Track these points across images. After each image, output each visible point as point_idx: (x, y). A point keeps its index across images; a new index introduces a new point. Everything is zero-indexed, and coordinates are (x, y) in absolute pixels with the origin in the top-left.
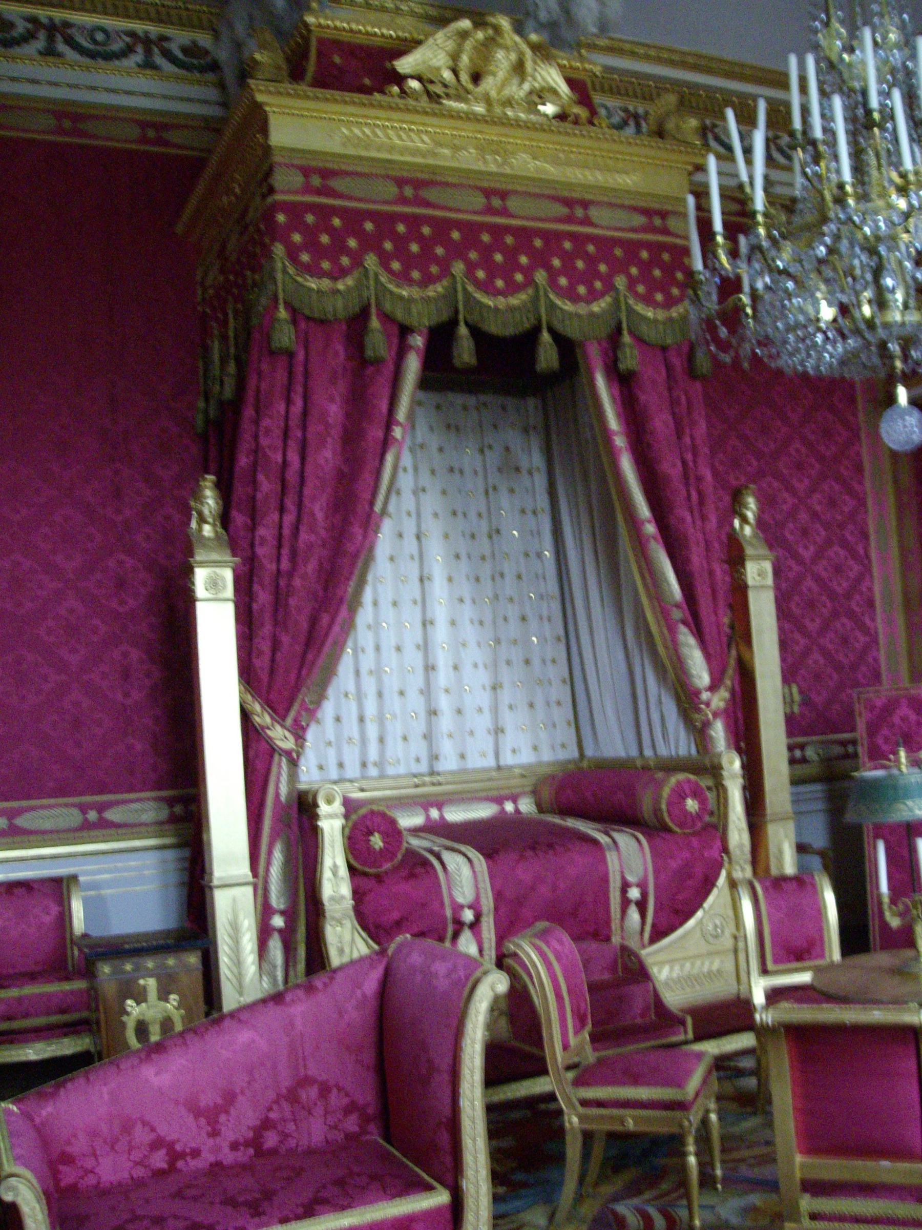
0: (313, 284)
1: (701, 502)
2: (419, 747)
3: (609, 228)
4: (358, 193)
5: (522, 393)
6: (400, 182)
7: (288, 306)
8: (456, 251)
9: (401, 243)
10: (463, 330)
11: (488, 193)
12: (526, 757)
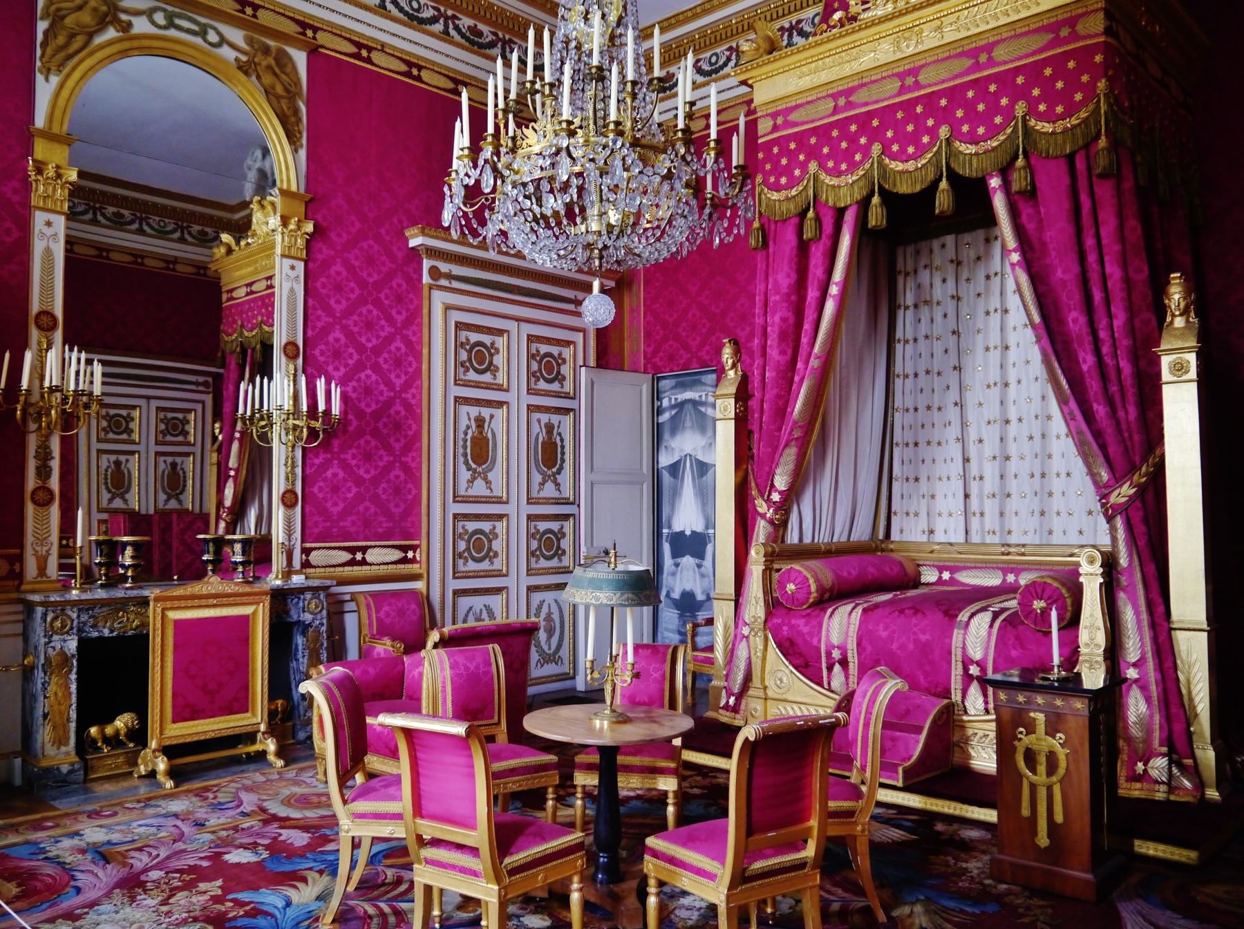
1: (1107, 302)
3: (1012, 61)
4: (804, 119)
6: (835, 96)
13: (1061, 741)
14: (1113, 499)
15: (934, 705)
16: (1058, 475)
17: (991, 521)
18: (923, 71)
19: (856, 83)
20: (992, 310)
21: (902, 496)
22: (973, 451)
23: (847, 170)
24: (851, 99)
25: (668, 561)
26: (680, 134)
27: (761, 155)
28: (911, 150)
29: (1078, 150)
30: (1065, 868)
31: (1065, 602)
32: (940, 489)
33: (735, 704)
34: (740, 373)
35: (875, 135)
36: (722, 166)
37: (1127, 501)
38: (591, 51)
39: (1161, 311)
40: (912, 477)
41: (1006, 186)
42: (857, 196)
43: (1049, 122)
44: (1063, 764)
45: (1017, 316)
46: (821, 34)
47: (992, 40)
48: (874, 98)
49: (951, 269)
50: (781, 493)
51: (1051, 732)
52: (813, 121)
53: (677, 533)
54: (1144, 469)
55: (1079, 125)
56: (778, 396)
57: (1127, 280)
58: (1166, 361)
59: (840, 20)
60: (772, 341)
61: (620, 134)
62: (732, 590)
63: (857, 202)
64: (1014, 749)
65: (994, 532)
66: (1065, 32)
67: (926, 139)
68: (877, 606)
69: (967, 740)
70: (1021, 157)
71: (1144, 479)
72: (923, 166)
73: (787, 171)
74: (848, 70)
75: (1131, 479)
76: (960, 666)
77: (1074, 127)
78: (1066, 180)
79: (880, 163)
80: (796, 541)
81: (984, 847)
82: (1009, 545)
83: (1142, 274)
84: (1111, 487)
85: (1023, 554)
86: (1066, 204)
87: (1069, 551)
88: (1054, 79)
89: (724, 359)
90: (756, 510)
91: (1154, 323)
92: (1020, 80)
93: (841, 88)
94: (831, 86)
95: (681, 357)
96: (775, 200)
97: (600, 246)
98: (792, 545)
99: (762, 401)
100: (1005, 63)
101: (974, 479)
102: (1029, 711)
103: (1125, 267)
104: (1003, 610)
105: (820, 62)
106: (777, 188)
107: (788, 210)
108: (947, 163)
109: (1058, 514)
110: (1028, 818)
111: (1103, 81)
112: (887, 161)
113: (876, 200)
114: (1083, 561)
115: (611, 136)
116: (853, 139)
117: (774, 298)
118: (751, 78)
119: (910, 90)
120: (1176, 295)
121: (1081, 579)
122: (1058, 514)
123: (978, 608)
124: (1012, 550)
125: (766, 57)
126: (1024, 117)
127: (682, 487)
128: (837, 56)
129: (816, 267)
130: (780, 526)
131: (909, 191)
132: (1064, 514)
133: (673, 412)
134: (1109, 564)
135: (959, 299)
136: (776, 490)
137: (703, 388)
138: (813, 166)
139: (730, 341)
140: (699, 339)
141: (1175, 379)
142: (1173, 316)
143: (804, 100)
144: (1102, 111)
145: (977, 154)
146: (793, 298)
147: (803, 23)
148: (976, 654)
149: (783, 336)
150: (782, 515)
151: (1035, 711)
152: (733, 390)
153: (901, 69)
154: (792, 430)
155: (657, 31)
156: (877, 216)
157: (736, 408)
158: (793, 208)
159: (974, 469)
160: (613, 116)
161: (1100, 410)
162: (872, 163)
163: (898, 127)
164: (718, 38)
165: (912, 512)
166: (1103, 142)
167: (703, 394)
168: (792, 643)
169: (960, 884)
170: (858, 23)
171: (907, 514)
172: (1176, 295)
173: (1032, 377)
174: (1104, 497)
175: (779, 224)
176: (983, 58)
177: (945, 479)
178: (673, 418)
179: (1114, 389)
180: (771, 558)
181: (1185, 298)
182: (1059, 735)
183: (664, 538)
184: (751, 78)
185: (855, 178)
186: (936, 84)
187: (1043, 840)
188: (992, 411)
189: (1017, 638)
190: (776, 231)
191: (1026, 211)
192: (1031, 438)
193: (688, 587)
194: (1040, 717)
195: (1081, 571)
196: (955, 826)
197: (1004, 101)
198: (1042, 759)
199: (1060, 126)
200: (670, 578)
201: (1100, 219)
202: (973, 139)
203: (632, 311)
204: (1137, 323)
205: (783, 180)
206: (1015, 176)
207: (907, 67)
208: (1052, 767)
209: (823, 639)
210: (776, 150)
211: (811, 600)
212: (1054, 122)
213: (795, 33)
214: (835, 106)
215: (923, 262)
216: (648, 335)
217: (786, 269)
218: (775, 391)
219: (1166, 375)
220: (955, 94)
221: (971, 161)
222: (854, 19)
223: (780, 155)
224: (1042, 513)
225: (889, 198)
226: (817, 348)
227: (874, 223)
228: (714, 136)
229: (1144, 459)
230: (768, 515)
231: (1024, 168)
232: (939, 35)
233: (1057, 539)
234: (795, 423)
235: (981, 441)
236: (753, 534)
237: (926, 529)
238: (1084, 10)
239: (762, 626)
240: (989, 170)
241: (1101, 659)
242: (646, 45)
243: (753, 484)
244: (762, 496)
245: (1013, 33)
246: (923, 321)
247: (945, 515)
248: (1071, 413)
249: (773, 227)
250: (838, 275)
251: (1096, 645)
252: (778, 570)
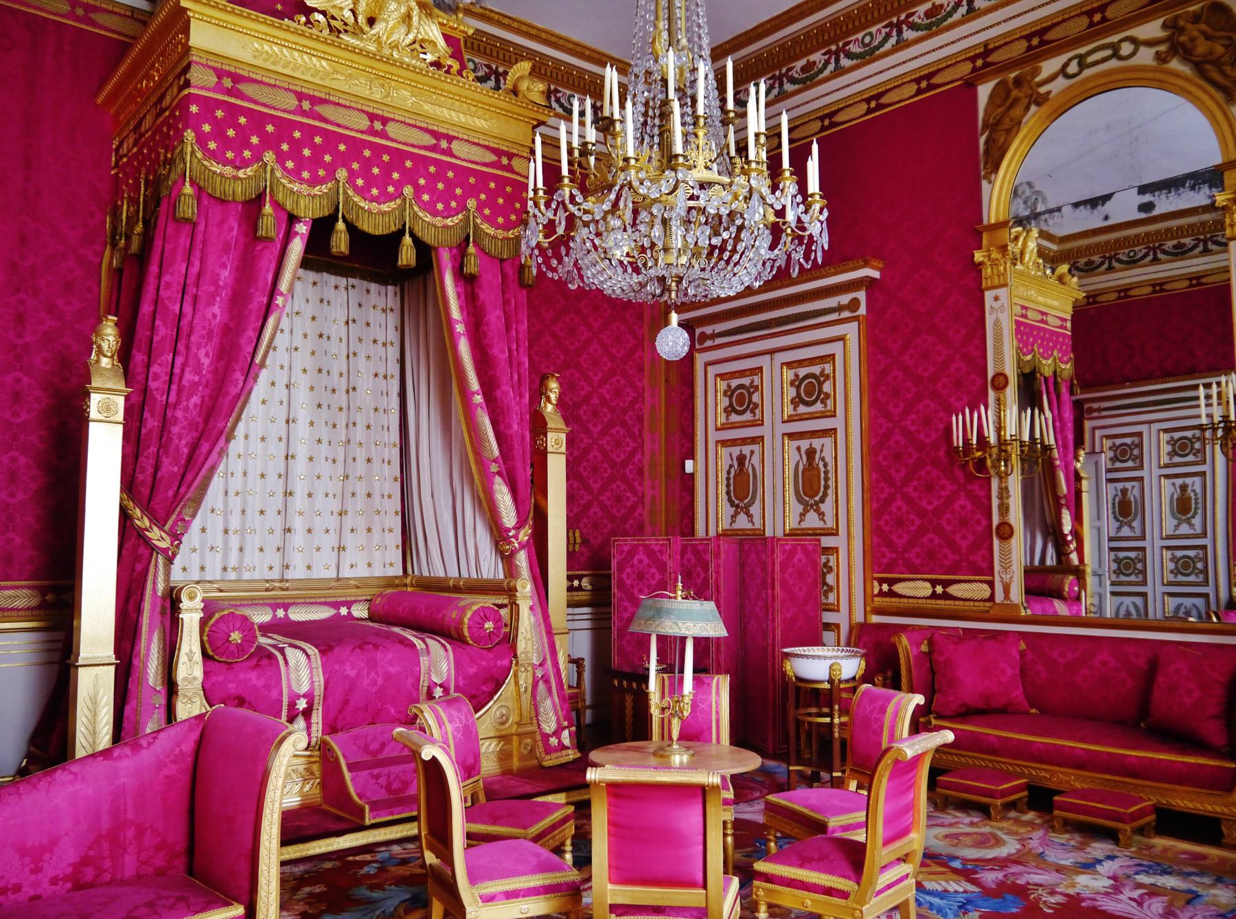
0: (217, 168)
2: (275, 559)
5: (383, 280)
6: (300, 96)
7: (192, 183)
8: (342, 160)
9: (296, 146)
10: (341, 225)
11: (372, 117)
12: (362, 572)
28: (375, 192)
85: (287, 589)
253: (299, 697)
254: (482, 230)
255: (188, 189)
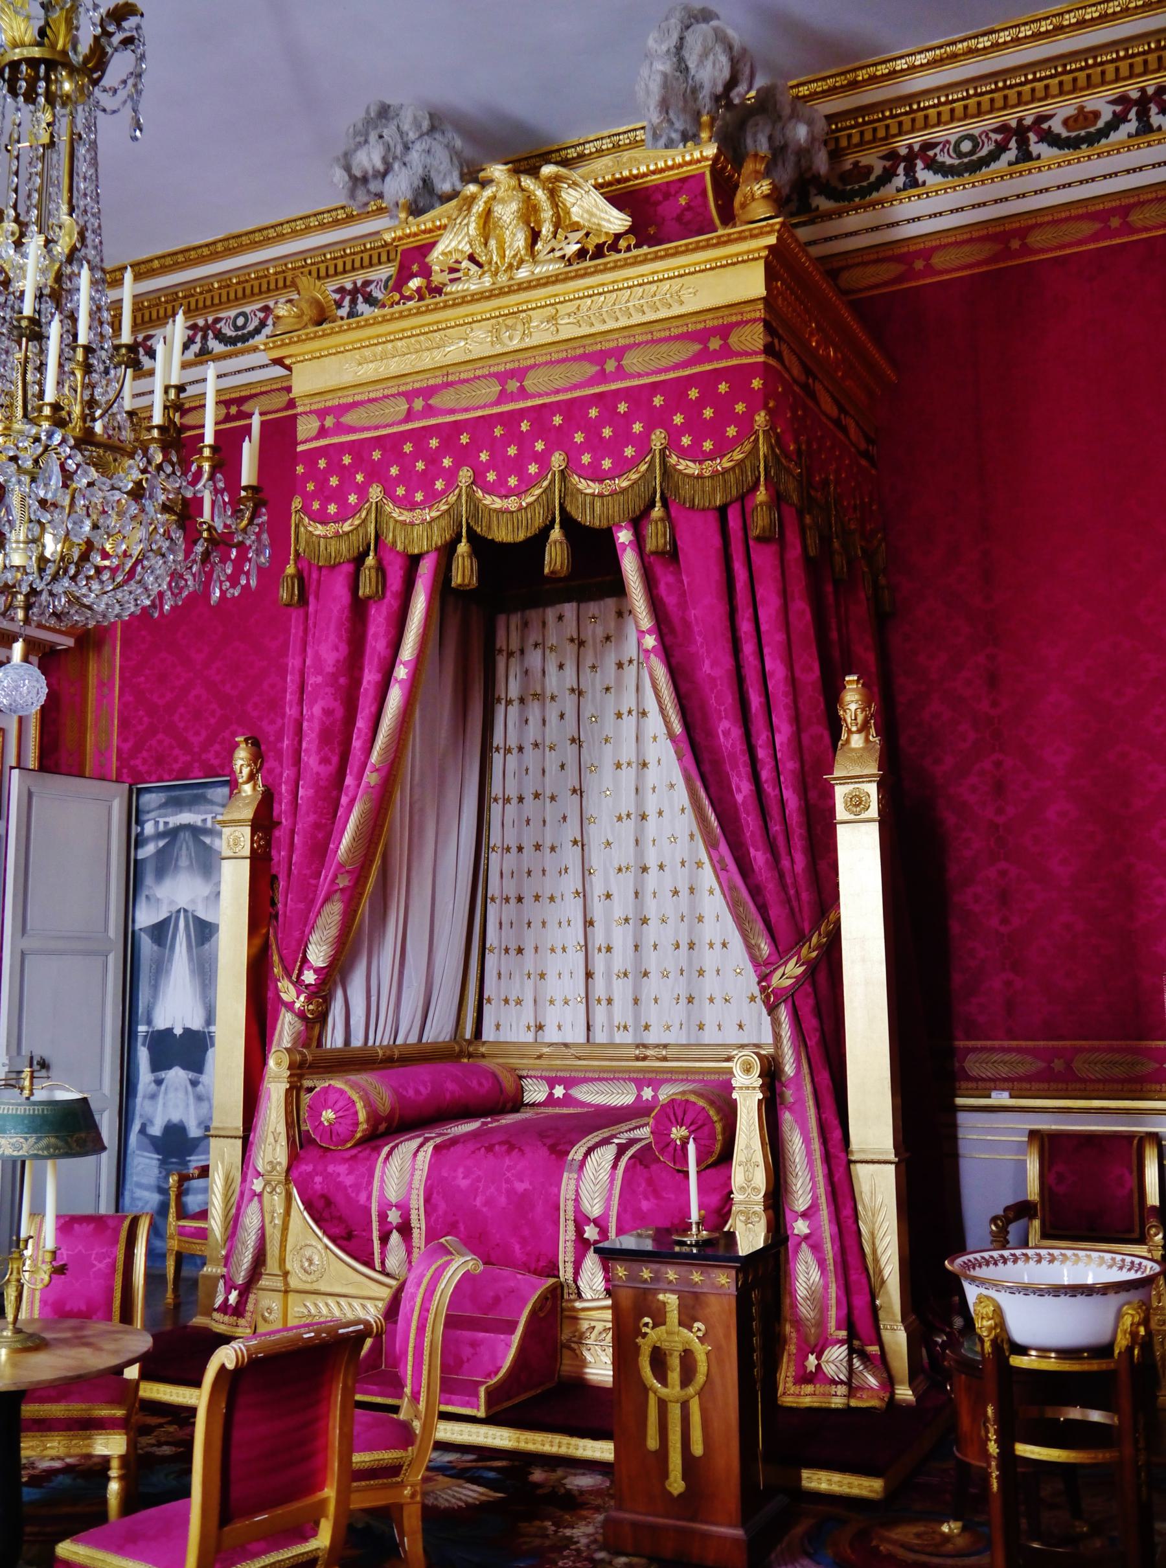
3: (648, 374)
6: (409, 396)
13: (700, 1334)
14: (777, 981)
15: (535, 1289)
16: (711, 945)
17: (622, 1011)
18: (531, 374)
19: (439, 381)
20: (625, 711)
21: (499, 975)
22: (598, 910)
23: (422, 502)
24: (431, 402)
25: (145, 1076)
26: (155, 433)
27: (300, 469)
28: (513, 481)
29: (731, 503)
30: (707, 1522)
31: (713, 1128)
32: (553, 964)
33: (238, 1303)
34: (260, 789)
35: (464, 456)
36: (221, 485)
37: (793, 984)
38: (22, 293)
39: (835, 725)
40: (513, 947)
41: (639, 542)
42: (438, 540)
43: (694, 462)
44: (702, 1368)
45: (654, 724)
46: (392, 306)
47: (622, 342)
48: (464, 404)
49: (571, 649)
50: (317, 971)
51: (686, 1321)
52: (377, 428)
53: (160, 1032)
54: (814, 940)
55: (733, 468)
56: (317, 826)
57: (793, 681)
58: (840, 792)
59: (419, 290)
60: (310, 741)
61: (60, 422)
62: (238, 1122)
63: (437, 549)
64: (637, 1348)
65: (625, 1027)
66: (715, 344)
67: (533, 469)
68: (455, 1141)
69: (580, 1338)
70: (658, 504)
71: (814, 954)
72: (529, 505)
73: (338, 496)
74: (428, 360)
75: (798, 953)
76: (571, 1227)
77: (726, 471)
78: (716, 541)
79: (470, 496)
80: (339, 1043)
81: (599, 1502)
82: (645, 1046)
83: (811, 675)
84: (772, 964)
85: (665, 1059)
86: (716, 573)
87: (725, 1053)
88: (701, 403)
89: (237, 768)
90: (279, 998)
91: (827, 740)
92: (658, 401)
93: (417, 385)
94: (403, 380)
95: (176, 760)
96: (319, 536)
97: (25, 589)
98: (333, 1050)
99: (293, 832)
100: (640, 375)
101: (600, 950)
102: (656, 1291)
103: (790, 665)
104: (632, 1142)
105: (390, 345)
106: (322, 518)
107: (338, 552)
108: (561, 505)
109: (711, 1000)
110: (656, 1452)
111: (763, 413)
112: (480, 494)
113: (463, 547)
114: (736, 1067)
115: (46, 425)
116: (433, 459)
117: (313, 680)
118: (290, 356)
119: (512, 398)
120: (852, 702)
121: (735, 1095)
122: (711, 1000)
123: (597, 1139)
124: (649, 1052)
125: (312, 329)
126: (662, 451)
127: (170, 960)
128: (413, 340)
129: (375, 635)
130: (314, 1022)
131: (509, 539)
132: (719, 1001)
133: (161, 844)
134: (771, 1073)
135: (580, 693)
136: (311, 967)
137: (209, 807)
138: (375, 492)
139: (246, 740)
140: (204, 734)
141: (852, 817)
142: (850, 732)
143: (365, 397)
144: (761, 454)
145: (601, 495)
146: (342, 680)
147: (372, 286)
148: (594, 1209)
149: (325, 737)
150: (319, 1005)
151: (665, 1291)
152: (248, 813)
153: (501, 368)
154: (335, 877)
155: (128, 276)
156: (463, 571)
157: (252, 842)
158: (345, 550)
159: (599, 936)
160: (50, 397)
161: (759, 857)
162: (460, 496)
163: (496, 447)
164: (248, 291)
165: (512, 998)
166: (761, 495)
167: (209, 817)
168: (328, 1202)
169: (560, 1564)
170: (443, 298)
171: (506, 1001)
172: (852, 702)
173: (678, 808)
174: (764, 978)
175: (324, 572)
176: (610, 366)
177: (559, 950)
178: (160, 852)
179: (776, 828)
180: (299, 1070)
181: (863, 710)
182: (697, 1325)
183: (140, 1040)
184: (290, 356)
185: (434, 514)
186: (547, 394)
187: (676, 1484)
188: (624, 853)
189: (650, 1182)
190: (319, 581)
191: (665, 579)
192: (676, 893)
193: (175, 1118)
194: (671, 1300)
195: (734, 1083)
196: (560, 1473)
197: (637, 427)
198: (675, 1362)
199: (708, 467)
200: (147, 1102)
201: (758, 597)
202: (598, 476)
203: (101, 685)
204: (806, 740)
205: (332, 509)
206: (650, 530)
207: (509, 366)
208: (687, 1378)
209: (375, 1194)
210: (322, 463)
211: (358, 1135)
212: (701, 463)
213: (360, 299)
214: (410, 410)
215: (533, 637)
216: (124, 724)
217: (333, 637)
218: (312, 818)
219: (841, 813)
220: (573, 409)
221: (593, 504)
222: (438, 291)
223: (329, 471)
224: (690, 1000)
225: (482, 546)
226: (375, 757)
227: (459, 581)
228: (209, 439)
229: (816, 926)
230: (297, 1005)
231: (662, 520)
232: (553, 328)
233: (710, 1036)
234: (340, 866)
235: (608, 896)
236: (273, 1035)
237: (532, 1024)
238: (739, 318)
239: (283, 1178)
240: (617, 520)
241: (759, 1208)
242: (112, 295)
243: (276, 958)
244: (288, 974)
245: (649, 337)
246: (531, 722)
247: (559, 1002)
248: (722, 860)
249: (315, 576)
250: (408, 652)
251: (754, 1188)
252: (310, 1090)
253: (390, 1206)
254: (680, 471)
255: (290, 569)
